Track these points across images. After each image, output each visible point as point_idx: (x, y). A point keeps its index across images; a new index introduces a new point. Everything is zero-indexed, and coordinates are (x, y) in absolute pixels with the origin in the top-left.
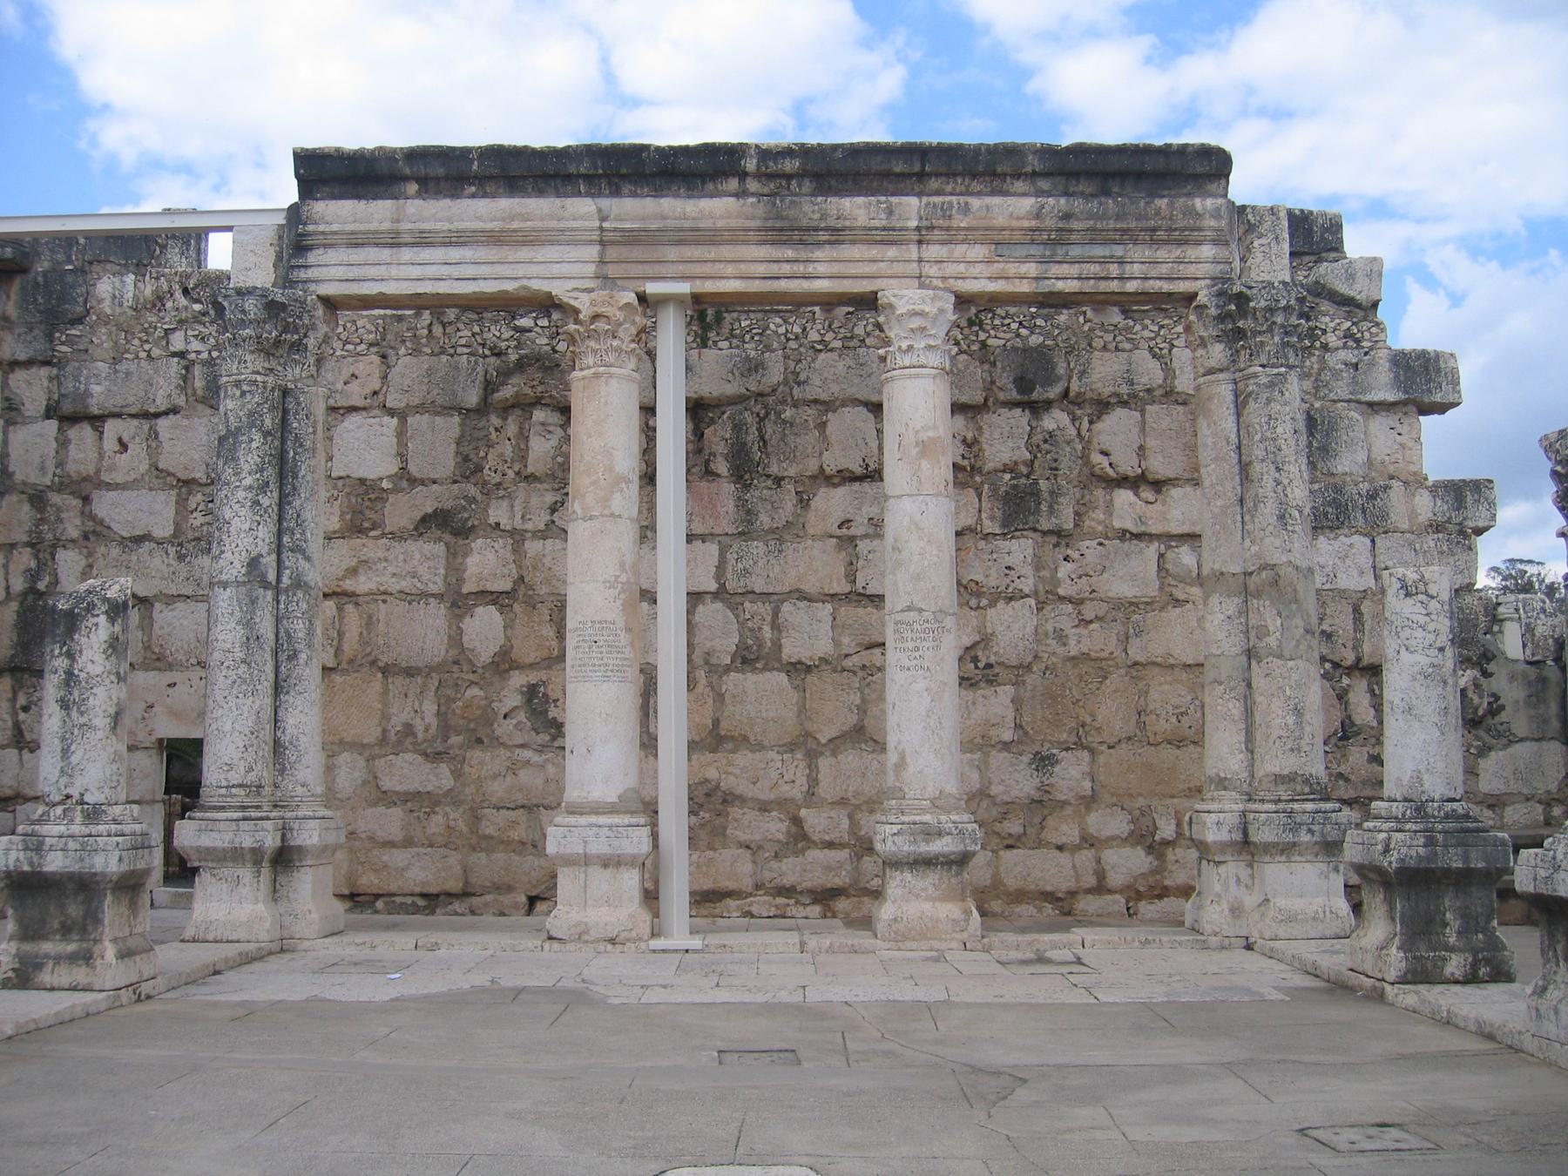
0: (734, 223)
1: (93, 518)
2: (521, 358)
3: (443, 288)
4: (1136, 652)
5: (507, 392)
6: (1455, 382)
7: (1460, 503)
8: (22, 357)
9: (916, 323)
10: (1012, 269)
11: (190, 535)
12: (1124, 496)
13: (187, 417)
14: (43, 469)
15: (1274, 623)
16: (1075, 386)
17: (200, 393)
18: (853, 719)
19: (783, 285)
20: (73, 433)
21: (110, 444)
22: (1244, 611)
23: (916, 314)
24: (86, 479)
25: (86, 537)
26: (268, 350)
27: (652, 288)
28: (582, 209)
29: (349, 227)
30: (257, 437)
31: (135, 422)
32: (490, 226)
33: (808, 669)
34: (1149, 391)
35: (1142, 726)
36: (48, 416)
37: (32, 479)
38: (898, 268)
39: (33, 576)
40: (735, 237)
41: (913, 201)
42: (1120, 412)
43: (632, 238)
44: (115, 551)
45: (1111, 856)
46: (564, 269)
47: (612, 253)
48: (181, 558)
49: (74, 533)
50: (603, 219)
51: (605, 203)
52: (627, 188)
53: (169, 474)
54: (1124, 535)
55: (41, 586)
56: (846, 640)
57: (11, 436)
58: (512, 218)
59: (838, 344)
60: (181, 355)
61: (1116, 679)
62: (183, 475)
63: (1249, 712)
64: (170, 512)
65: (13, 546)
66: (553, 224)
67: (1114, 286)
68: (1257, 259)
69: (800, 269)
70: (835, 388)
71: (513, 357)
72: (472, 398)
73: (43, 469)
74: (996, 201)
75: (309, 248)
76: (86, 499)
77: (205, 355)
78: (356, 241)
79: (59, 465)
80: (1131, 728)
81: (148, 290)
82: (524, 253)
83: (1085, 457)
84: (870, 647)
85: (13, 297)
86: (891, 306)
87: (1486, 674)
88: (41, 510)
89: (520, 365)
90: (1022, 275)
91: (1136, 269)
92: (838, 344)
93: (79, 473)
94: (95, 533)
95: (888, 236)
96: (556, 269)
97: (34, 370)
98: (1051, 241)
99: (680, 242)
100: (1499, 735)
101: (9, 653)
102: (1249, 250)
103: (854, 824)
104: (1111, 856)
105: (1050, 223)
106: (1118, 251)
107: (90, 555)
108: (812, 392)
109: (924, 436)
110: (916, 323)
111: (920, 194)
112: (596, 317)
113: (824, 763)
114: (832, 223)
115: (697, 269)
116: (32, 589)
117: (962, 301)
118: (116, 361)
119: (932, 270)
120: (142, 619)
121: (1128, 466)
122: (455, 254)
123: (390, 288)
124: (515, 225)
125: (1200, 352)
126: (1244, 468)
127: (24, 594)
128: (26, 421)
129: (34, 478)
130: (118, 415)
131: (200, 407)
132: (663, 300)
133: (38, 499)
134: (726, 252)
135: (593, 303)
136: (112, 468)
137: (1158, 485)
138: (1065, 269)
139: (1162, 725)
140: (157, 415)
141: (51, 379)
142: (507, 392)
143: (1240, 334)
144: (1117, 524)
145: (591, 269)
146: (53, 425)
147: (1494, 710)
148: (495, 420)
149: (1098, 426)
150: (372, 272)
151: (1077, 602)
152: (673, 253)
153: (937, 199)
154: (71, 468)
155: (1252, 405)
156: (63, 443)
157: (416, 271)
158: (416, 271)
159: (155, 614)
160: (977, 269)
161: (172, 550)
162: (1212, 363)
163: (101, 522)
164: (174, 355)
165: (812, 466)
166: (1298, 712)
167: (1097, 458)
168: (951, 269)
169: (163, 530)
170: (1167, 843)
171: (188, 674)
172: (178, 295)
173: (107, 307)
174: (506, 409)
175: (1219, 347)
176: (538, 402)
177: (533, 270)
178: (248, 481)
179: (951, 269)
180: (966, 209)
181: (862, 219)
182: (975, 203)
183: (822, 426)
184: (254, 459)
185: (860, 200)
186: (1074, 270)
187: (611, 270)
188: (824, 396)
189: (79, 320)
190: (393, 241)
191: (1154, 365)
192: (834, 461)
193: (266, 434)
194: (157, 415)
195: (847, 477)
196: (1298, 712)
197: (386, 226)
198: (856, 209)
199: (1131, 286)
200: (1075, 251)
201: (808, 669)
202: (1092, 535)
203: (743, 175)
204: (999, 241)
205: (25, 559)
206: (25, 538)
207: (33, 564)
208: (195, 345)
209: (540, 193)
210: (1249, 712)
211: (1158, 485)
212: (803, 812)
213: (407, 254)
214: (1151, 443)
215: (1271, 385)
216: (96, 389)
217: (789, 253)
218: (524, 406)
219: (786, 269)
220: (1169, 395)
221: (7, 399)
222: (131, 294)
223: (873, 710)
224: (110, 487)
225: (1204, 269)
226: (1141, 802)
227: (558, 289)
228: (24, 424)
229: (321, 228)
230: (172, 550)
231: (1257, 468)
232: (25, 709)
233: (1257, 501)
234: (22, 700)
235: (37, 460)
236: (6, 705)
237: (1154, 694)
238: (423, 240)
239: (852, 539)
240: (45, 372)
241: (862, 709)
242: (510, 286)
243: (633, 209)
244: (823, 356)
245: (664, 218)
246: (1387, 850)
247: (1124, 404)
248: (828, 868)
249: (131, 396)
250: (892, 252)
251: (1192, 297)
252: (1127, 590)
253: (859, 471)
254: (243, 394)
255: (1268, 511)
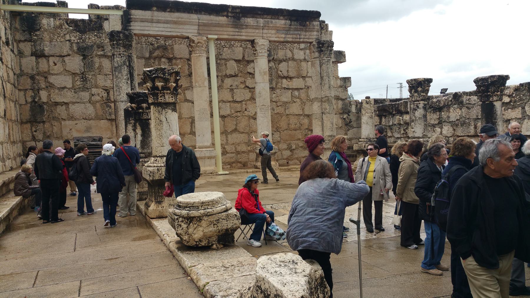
0: (226, 23)
1: (49, 82)
2: (158, 46)
3: (163, 33)
4: (287, 112)
5: (155, 54)
6: (345, 57)
7: (345, 82)
8: (23, 39)
9: (263, 47)
10: (280, 36)
11: (77, 87)
12: (284, 81)
13: (73, 57)
14: (33, 69)
15: (328, 107)
16: (275, 57)
17: (76, 51)
18: (235, 127)
19: (236, 37)
20: (40, 60)
21: (51, 63)
22: (321, 105)
23: (263, 45)
24: (45, 72)
25: (47, 87)
26: (124, 47)
27: (210, 36)
28: (194, 17)
29: (141, 17)
30: (126, 67)
31: (58, 58)
32: (174, 19)
33: (225, 117)
34: (289, 58)
35: (288, 127)
36: (32, 55)
37: (30, 72)
38: (258, 35)
39: (34, 98)
40: (227, 26)
41: (262, 20)
42: (284, 63)
43: (205, 25)
44: (57, 91)
45: (284, 152)
46: (191, 31)
47: (201, 28)
48: (75, 92)
49: (44, 87)
50: (199, 20)
51: (199, 16)
52: (203, 13)
53: (69, 71)
54: (285, 88)
55: (36, 100)
56: (232, 111)
57: (22, 61)
58: (179, 18)
59: (228, 46)
60: (69, 41)
61: (284, 118)
62: (74, 72)
63: (323, 124)
64: (71, 81)
65: (26, 90)
66: (188, 20)
67: (298, 40)
68: (323, 35)
69: (239, 33)
70: (228, 56)
71: (156, 46)
72: (147, 55)
73: (33, 69)
74: (277, 21)
75: (131, 21)
76: (46, 78)
77: (76, 41)
78: (142, 21)
79: (37, 68)
80: (287, 127)
81: (58, 23)
82: (181, 26)
83: (277, 72)
84: (237, 112)
85: (17, 22)
86: (258, 43)
87: (349, 115)
88: (34, 80)
89: (158, 48)
90: (281, 37)
91: (302, 36)
92: (228, 46)
93: (43, 71)
94: (50, 86)
95: (257, 28)
96: (189, 31)
97: (26, 43)
98: (287, 31)
99: (215, 26)
100: (351, 127)
101: (29, 117)
102: (322, 33)
103: (236, 148)
104: (284, 152)
105: (288, 26)
106: (299, 32)
107: (49, 92)
108: (224, 56)
109: (265, 71)
110: (263, 47)
111: (262, 18)
112: (198, 43)
113: (229, 136)
114: (246, 24)
115: (219, 33)
116: (34, 101)
117: (270, 41)
118: (51, 42)
119: (265, 35)
120: (66, 108)
121: (286, 74)
122: (166, 25)
123: (151, 33)
124: (180, 20)
125: (313, 54)
126: (322, 78)
127: (32, 102)
128: (26, 57)
129: (30, 71)
130: (53, 56)
131: (76, 55)
132: (211, 39)
133: (32, 78)
134: (225, 29)
135: (198, 39)
136: (53, 70)
137: (291, 78)
138: (289, 36)
139: (293, 126)
140: (64, 56)
141: (32, 46)
142: (155, 54)
143: (322, 51)
144: (283, 86)
145: (196, 31)
146: (34, 58)
147: (350, 122)
148: (152, 61)
149: (280, 66)
150: (147, 28)
151: (276, 102)
152: (214, 29)
153: (266, 20)
154: (40, 69)
155: (324, 65)
156: (38, 63)
157: (157, 29)
158: (157, 29)
159: (70, 107)
160: (273, 36)
161: (73, 91)
162: (315, 56)
163: (51, 84)
164: (67, 41)
165: (224, 73)
166: (332, 124)
167: (279, 72)
168: (269, 35)
169: (70, 85)
170: (294, 149)
171: (81, 121)
172: (66, 24)
173: (46, 27)
174: (155, 58)
175: (317, 53)
176: (162, 57)
177: (184, 31)
178: (125, 78)
179: (269, 35)
180: (272, 22)
181: (252, 24)
182: (274, 21)
183: (226, 65)
184: (126, 72)
185: (251, 19)
186: (291, 36)
187: (201, 32)
188: (226, 58)
189: (39, 30)
190: (152, 21)
191: (290, 53)
192: (229, 72)
193: (127, 66)
194: (64, 56)
195: (231, 76)
196: (332, 124)
197: (150, 18)
198: (250, 21)
199: (301, 40)
200: (291, 32)
201: (225, 117)
202: (279, 88)
203: (228, 12)
204: (278, 30)
205: (30, 93)
206: (30, 88)
207: (33, 94)
208: (73, 38)
209: (184, 12)
210: (323, 124)
211: (291, 78)
212: (226, 147)
213: (154, 25)
214: (290, 69)
215: (328, 61)
216: (46, 49)
217: (237, 30)
218: (159, 58)
219: (237, 33)
220: (293, 59)
221: (19, 50)
222: (53, 24)
223: (239, 125)
224: (53, 74)
225: (315, 37)
226: (289, 142)
227: (190, 36)
228: (25, 57)
229: (134, 17)
230: (73, 91)
231: (325, 77)
232: (36, 131)
233: (325, 84)
234: (34, 129)
235: (31, 67)
236: (29, 131)
237: (291, 121)
238: (158, 22)
239: (233, 89)
240: (29, 43)
241: (236, 125)
242: (179, 34)
243: (205, 18)
244: (225, 49)
245: (212, 20)
246: (365, 147)
247: (285, 61)
248: (231, 158)
249: (57, 51)
250: (257, 31)
251: (311, 43)
252: (285, 100)
253: (234, 75)
254: (121, 57)
255: (327, 86)
